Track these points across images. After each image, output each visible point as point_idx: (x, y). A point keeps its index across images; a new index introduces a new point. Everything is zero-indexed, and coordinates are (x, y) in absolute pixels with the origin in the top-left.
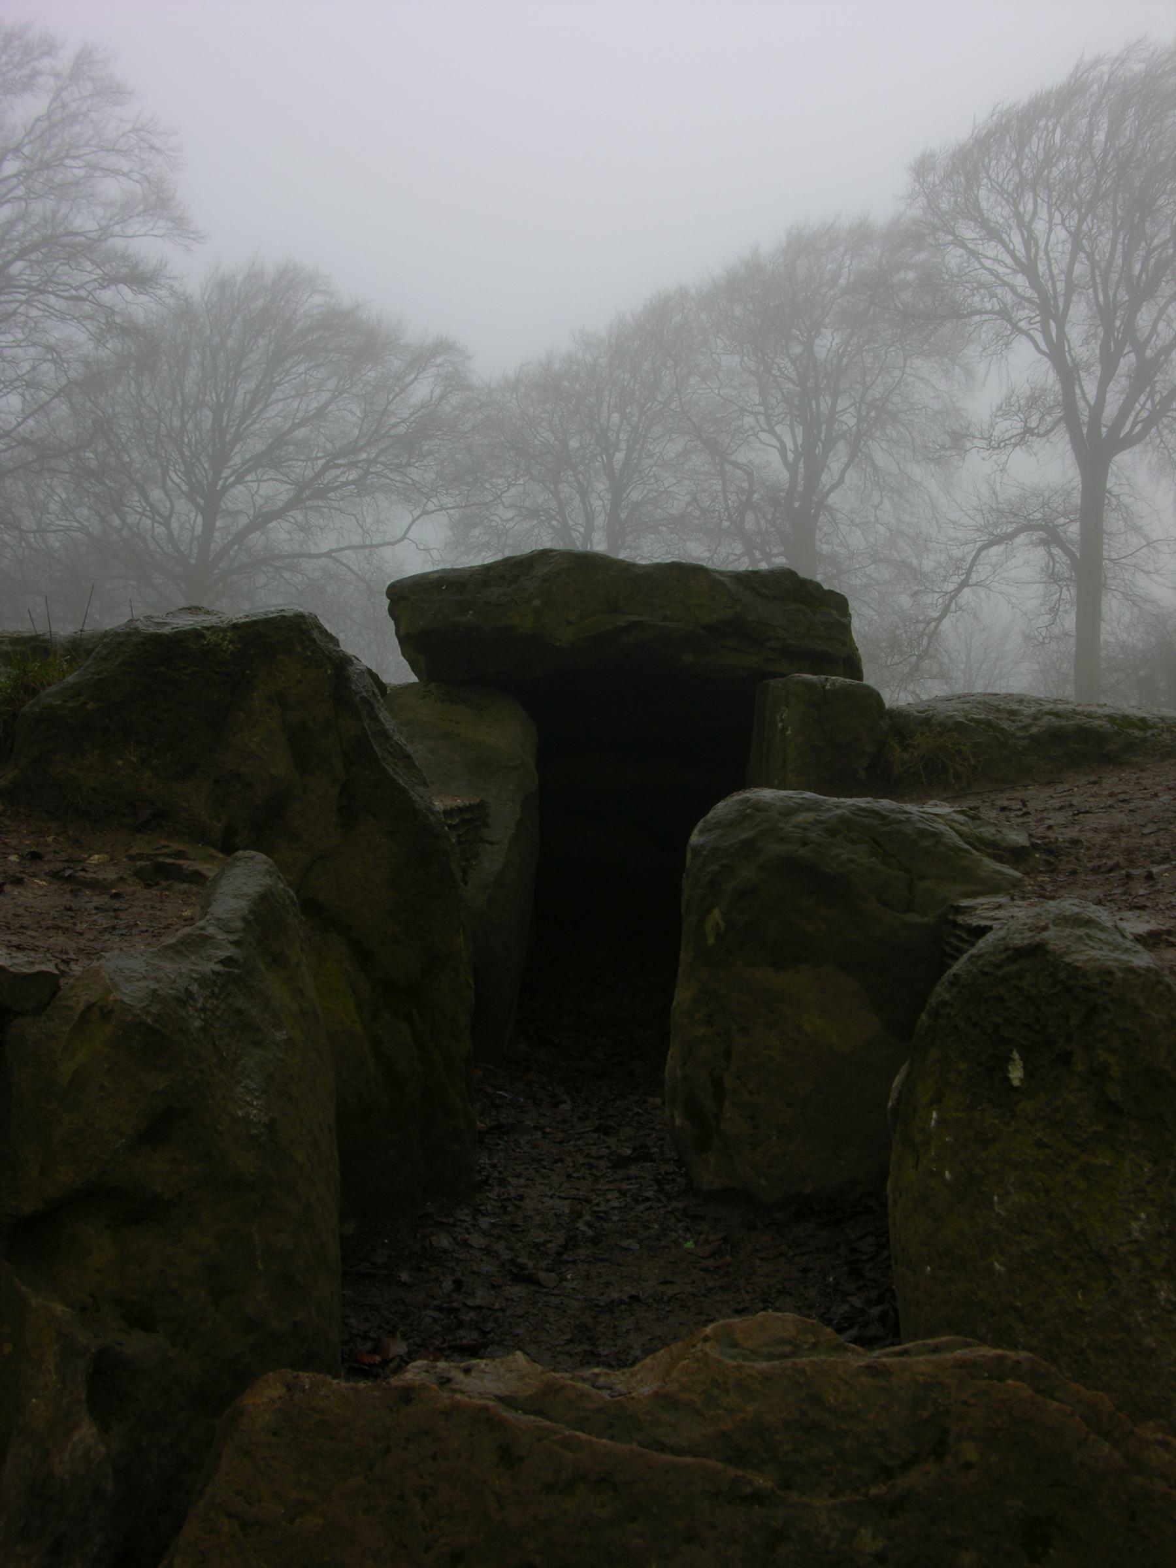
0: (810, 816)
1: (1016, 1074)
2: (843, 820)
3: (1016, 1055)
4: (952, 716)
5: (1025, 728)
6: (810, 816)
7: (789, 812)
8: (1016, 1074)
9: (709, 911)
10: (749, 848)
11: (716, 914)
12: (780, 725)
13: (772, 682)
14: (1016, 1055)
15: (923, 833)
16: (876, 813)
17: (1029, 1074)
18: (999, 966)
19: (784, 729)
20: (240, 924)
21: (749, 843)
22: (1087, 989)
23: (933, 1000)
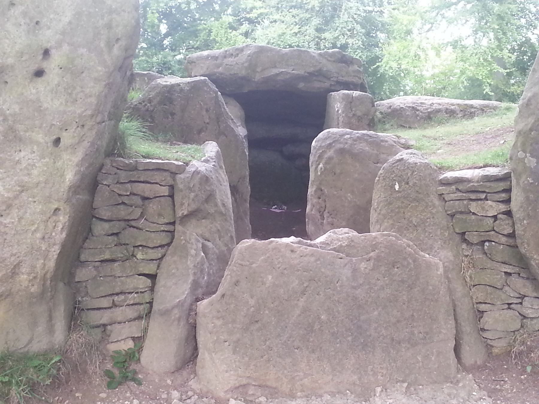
0: (348, 136)
1: (397, 187)
2: (358, 137)
3: (397, 183)
4: (399, 106)
5: (427, 109)
6: (348, 136)
7: (342, 135)
8: (397, 187)
9: (319, 164)
10: (330, 146)
11: (321, 165)
12: (337, 110)
13: (333, 93)
14: (397, 183)
15: (382, 141)
16: (368, 135)
17: (400, 187)
18: (393, 164)
19: (338, 111)
20: (214, 157)
21: (330, 144)
22: (412, 167)
23: (379, 173)
